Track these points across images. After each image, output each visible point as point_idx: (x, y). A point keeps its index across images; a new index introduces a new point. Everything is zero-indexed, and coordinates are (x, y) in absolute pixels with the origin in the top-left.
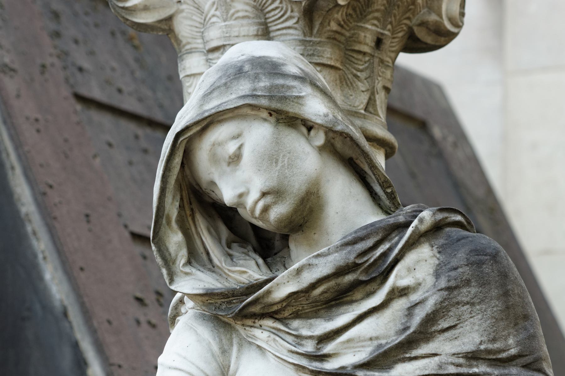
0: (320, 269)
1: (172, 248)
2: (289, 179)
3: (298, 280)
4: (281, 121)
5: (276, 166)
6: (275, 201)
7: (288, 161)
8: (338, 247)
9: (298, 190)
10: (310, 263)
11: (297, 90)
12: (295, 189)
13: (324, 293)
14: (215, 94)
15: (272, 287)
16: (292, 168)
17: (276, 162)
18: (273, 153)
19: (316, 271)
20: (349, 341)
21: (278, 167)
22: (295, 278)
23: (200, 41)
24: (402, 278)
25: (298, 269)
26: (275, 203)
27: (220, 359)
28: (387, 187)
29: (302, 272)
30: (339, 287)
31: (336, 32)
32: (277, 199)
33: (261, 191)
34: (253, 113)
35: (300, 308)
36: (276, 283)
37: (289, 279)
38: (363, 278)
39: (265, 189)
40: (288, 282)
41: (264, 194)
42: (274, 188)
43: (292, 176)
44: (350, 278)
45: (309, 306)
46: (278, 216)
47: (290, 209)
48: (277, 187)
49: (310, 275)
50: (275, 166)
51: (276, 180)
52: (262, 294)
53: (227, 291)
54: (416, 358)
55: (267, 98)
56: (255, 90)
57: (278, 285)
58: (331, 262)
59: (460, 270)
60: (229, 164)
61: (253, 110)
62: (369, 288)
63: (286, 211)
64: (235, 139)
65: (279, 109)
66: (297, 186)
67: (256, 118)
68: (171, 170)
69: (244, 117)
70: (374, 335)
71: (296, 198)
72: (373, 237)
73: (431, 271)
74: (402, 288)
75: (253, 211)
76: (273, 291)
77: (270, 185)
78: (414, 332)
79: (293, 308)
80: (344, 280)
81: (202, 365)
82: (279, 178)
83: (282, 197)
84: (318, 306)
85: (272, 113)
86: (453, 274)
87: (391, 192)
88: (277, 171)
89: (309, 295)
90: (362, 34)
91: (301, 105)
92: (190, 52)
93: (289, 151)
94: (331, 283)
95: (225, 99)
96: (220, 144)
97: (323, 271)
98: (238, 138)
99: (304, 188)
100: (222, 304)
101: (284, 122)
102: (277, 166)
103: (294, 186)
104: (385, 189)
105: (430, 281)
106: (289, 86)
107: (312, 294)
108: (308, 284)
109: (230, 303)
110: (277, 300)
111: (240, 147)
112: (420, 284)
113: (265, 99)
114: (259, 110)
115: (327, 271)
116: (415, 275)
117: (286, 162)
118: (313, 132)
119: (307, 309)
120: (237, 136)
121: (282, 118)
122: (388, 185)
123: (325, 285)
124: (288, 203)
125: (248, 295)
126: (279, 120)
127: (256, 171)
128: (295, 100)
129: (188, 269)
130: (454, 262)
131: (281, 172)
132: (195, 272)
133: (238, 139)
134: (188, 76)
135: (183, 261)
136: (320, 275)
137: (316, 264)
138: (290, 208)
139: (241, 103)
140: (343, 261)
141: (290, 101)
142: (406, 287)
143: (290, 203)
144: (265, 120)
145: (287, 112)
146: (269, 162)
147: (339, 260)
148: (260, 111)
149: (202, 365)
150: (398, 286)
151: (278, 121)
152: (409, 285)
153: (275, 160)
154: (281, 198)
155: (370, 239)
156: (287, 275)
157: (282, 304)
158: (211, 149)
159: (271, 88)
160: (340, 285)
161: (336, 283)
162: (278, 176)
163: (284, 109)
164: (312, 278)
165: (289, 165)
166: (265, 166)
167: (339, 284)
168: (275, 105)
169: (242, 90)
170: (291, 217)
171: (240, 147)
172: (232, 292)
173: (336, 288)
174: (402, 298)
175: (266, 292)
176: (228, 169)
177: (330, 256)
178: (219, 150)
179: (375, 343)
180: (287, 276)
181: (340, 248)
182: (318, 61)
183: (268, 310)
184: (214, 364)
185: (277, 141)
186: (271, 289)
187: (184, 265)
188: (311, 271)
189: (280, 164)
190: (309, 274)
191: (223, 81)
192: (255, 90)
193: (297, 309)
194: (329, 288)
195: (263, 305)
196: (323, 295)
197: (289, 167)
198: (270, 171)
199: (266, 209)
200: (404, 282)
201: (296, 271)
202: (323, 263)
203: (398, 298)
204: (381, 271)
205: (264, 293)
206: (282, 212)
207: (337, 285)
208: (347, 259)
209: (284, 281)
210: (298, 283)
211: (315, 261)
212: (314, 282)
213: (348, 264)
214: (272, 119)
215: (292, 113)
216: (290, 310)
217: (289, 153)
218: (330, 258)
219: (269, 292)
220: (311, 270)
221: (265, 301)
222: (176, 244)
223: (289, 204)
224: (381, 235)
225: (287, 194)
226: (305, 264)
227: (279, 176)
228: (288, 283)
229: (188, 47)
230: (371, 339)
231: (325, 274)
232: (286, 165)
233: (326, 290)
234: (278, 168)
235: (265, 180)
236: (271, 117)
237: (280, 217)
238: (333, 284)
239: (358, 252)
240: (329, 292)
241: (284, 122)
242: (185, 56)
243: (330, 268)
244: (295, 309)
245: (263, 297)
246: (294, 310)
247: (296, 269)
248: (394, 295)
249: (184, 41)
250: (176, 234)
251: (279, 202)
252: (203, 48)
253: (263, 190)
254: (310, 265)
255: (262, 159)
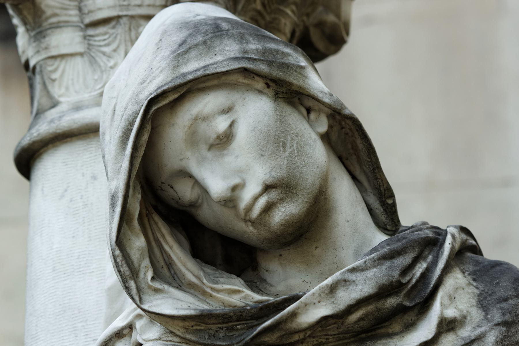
0: (360, 287)
1: (135, 255)
2: (301, 170)
3: (333, 300)
4: (280, 96)
5: (284, 152)
6: (283, 198)
7: (297, 147)
8: (375, 261)
9: (312, 185)
10: (346, 279)
11: (293, 59)
12: (308, 183)
13: (361, 319)
14: (193, 54)
15: (298, 308)
16: (302, 156)
17: (284, 147)
18: (278, 133)
19: (354, 290)
21: (286, 153)
22: (328, 297)
23: (75, 12)
25: (331, 286)
26: (282, 200)
28: (388, 196)
29: (337, 290)
30: (380, 313)
31: (259, 13)
32: (285, 195)
33: (264, 183)
34: (246, 81)
35: (324, 341)
36: (304, 302)
37: (320, 298)
38: (407, 303)
39: (269, 182)
40: (319, 302)
41: (267, 188)
42: (283, 180)
43: (304, 166)
44: (393, 302)
45: (335, 338)
46: (287, 218)
47: (303, 209)
48: (287, 179)
49: (347, 294)
50: (283, 151)
51: (284, 169)
52: (285, 317)
53: (233, 312)
55: (265, 63)
57: (306, 306)
58: (371, 279)
59: (510, 302)
60: (211, 147)
62: (408, 317)
63: (299, 212)
64: (224, 113)
65: (282, 78)
67: (249, 88)
68: (138, 148)
69: (233, 86)
71: (309, 196)
72: (410, 251)
73: (473, 302)
74: (449, 319)
75: (250, 208)
76: (299, 313)
77: (277, 175)
79: (314, 340)
80: (385, 304)
82: (288, 167)
83: (293, 193)
84: (345, 338)
85: (271, 84)
86: (504, 305)
87: (392, 203)
88: (285, 159)
89: (343, 321)
90: (283, 21)
91: (304, 77)
92: (57, 26)
93: (296, 135)
94: (371, 307)
95: (208, 61)
96: (205, 119)
97: (364, 290)
98: (228, 112)
99: (317, 183)
100: (218, 330)
101: (284, 98)
102: (285, 152)
103: (307, 179)
104: (386, 199)
105: (476, 314)
106: (284, 53)
107: (347, 321)
108: (346, 305)
109: (231, 329)
110: (304, 326)
112: (465, 317)
113: (264, 64)
114: (254, 79)
115: (369, 291)
116: (457, 306)
117: (295, 148)
119: (331, 342)
120: (228, 110)
121: (282, 92)
122: (390, 194)
123: (363, 309)
124: (300, 201)
125: (268, 316)
126: (278, 93)
127: (258, 157)
128: (298, 70)
129: (157, 285)
130: (501, 293)
131: (290, 159)
132: (168, 289)
133: (228, 114)
134: (54, 57)
135: (150, 274)
136: (360, 295)
137: (353, 280)
138: (304, 208)
139: (236, 65)
140: (385, 278)
141: (292, 70)
142: (453, 319)
143: (303, 201)
144: (261, 92)
145: (291, 84)
146: (275, 145)
147: (381, 277)
148: (254, 80)
150: (446, 317)
152: (455, 317)
153: (282, 143)
154: (291, 194)
155: (407, 254)
156: (319, 292)
157: (306, 333)
158: (192, 125)
159: (265, 52)
160: (381, 310)
161: (377, 308)
162: (287, 164)
163: (287, 80)
164: (350, 298)
165: (298, 152)
166: (270, 150)
167: (380, 309)
168: (276, 73)
169: (230, 51)
170: (303, 219)
171: (232, 125)
172: (240, 314)
173: (376, 314)
174: (450, 333)
175: (290, 314)
176: (209, 155)
177: (368, 272)
178: (203, 127)
180: (319, 294)
181: (377, 262)
183: (286, 340)
185: (281, 120)
186: (297, 311)
188: (347, 289)
189: (288, 150)
190: (346, 293)
191: (200, 38)
192: (246, 52)
193: (320, 341)
194: (368, 314)
195: (284, 333)
196: (359, 323)
197: (299, 154)
198: (277, 157)
199: (269, 208)
200: (451, 313)
201: (329, 289)
202: (362, 280)
203: (446, 333)
204: (424, 296)
205: (288, 315)
206: (293, 212)
207: (377, 311)
208: (390, 276)
209: (315, 301)
210: (332, 305)
211: (352, 277)
212: (353, 303)
213: (392, 282)
214: (270, 92)
215: (296, 85)
216: (309, 343)
217: (297, 136)
218: (370, 273)
219: (294, 315)
220: (347, 287)
221: (287, 327)
222: (139, 250)
223: (302, 203)
224: (417, 250)
225: (300, 189)
226: (340, 279)
227: (288, 165)
228: (319, 303)
229: (54, 20)
231: (366, 294)
232: (296, 151)
233: (364, 316)
234: (287, 154)
235: (271, 169)
236: (268, 90)
237: (290, 218)
238: (373, 308)
239: (400, 268)
240: (366, 319)
241: (284, 98)
242: (49, 31)
243: (372, 287)
244: (317, 341)
245: (285, 321)
246: (315, 343)
247: (330, 286)
248: (442, 328)
249: (49, 12)
250: (138, 236)
251: (288, 199)
252: (78, 22)
253: (267, 182)
254: (345, 281)
255: (267, 141)
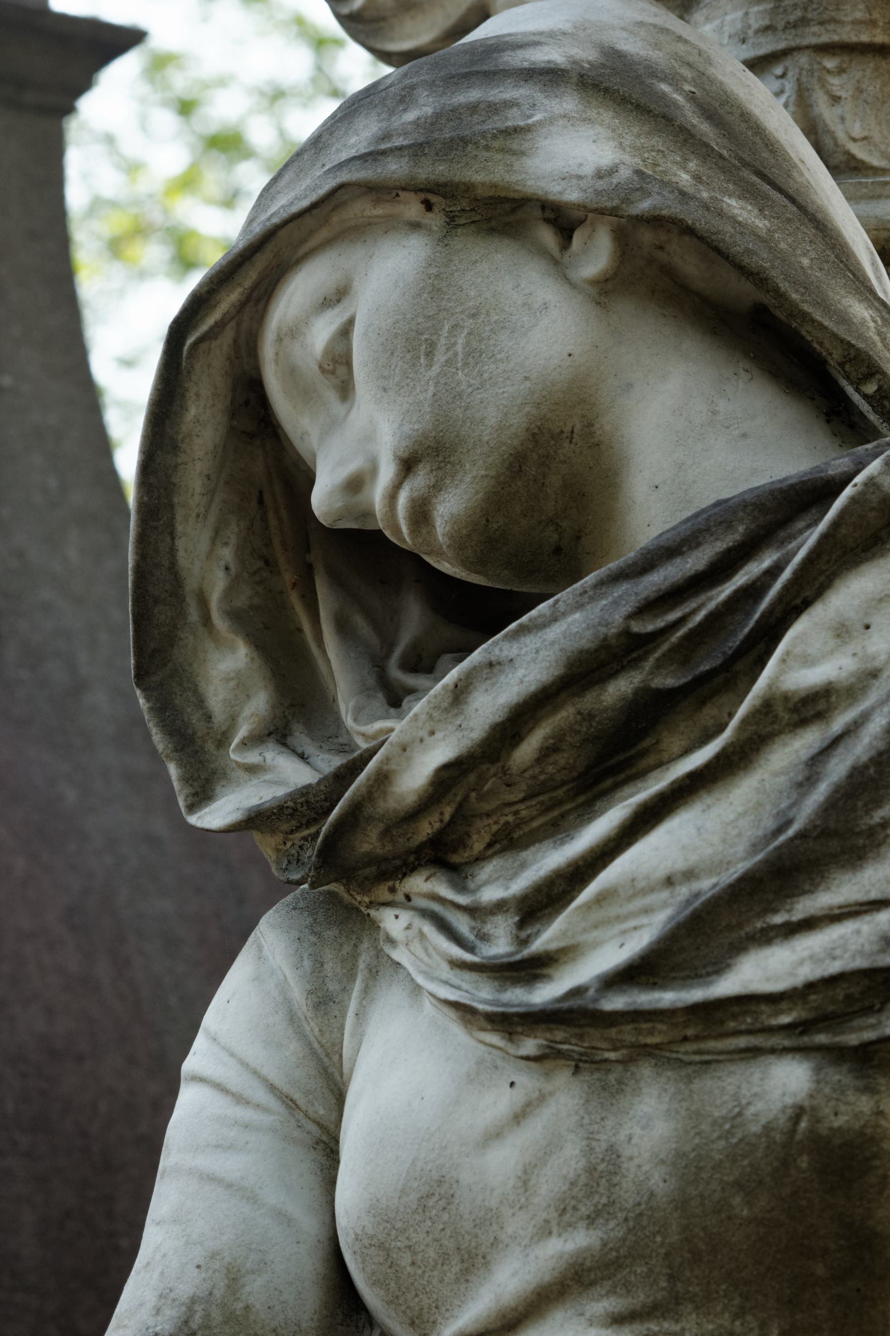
0: (520, 673)
1: (215, 695)
2: (468, 400)
3: (458, 722)
4: (462, 221)
5: (430, 366)
6: (437, 481)
7: (468, 343)
8: (586, 592)
9: (497, 430)
10: (493, 659)
11: (519, 113)
12: (486, 429)
13: (546, 753)
15: (387, 760)
16: (477, 363)
17: (429, 354)
18: (418, 324)
19: (507, 683)
20: (601, 899)
21: (433, 369)
22: (450, 715)
24: (808, 661)
25: (456, 686)
26: (437, 487)
27: (312, 1028)
28: (860, 376)
29: (470, 693)
30: (594, 724)
32: (440, 473)
33: (396, 456)
34: (379, 211)
35: (510, 818)
36: (396, 743)
37: (432, 723)
38: (668, 681)
40: (432, 733)
42: (426, 438)
43: (478, 389)
44: (623, 689)
45: (532, 806)
46: (447, 529)
47: (474, 499)
48: (433, 434)
49: (490, 698)
50: (427, 366)
51: (428, 410)
52: (364, 789)
53: (290, 799)
54: (809, 924)
55: (406, 152)
56: (386, 136)
57: (404, 750)
58: (553, 643)
61: (377, 202)
63: (466, 507)
64: (330, 306)
65: (442, 180)
66: (492, 416)
68: (180, 445)
70: (680, 865)
71: (490, 460)
72: (712, 539)
74: (803, 694)
76: (393, 771)
77: (414, 430)
78: (802, 835)
79: (491, 821)
80: (603, 698)
81: (256, 1055)
82: (436, 401)
83: (453, 465)
84: (560, 803)
85: (433, 199)
87: (877, 391)
88: (431, 382)
89: (503, 767)
91: (515, 154)
93: (474, 311)
97: (527, 679)
98: (339, 301)
99: (518, 421)
100: (303, 844)
101: (474, 222)
102: (431, 366)
103: (483, 419)
104: (858, 384)
106: (495, 104)
107: (511, 762)
108: (487, 727)
110: (411, 800)
111: (346, 331)
113: (402, 156)
114: (398, 198)
115: (539, 676)
116: (863, 647)
117: (459, 348)
118: (578, 239)
119: (533, 819)
121: (463, 210)
122: (864, 370)
123: (544, 725)
124: (468, 479)
126: (453, 217)
127: (379, 396)
128: (496, 144)
131: (442, 381)
132: (273, 760)
133: (340, 304)
136: (518, 694)
137: (510, 658)
138: (477, 492)
140: (589, 634)
141: (477, 147)
142: (818, 689)
143: (475, 478)
145: (469, 187)
146: (408, 356)
147: (578, 632)
148: (398, 201)
149: (256, 1055)
150: (787, 692)
151: (452, 223)
152: (830, 683)
153: (424, 347)
154: (449, 466)
155: (701, 549)
156: (427, 710)
157: (442, 814)
158: (277, 354)
160: (595, 716)
161: (579, 713)
162: (433, 396)
163: (457, 179)
164: (496, 707)
165: (468, 355)
166: (397, 372)
167: (589, 714)
169: (354, 145)
170: (485, 522)
171: (346, 331)
172: (303, 799)
173: (585, 729)
174: (808, 729)
175: (373, 778)
177: (558, 624)
179: (683, 891)
180: (428, 713)
181: (591, 593)
182: (825, 39)
183: (408, 840)
184: (294, 1048)
186: (385, 767)
187: (255, 740)
188: (493, 685)
189: (440, 357)
190: (490, 695)
193: (502, 822)
194: (562, 732)
195: (382, 826)
196: (551, 760)
197: (470, 360)
198: (412, 384)
201: (450, 694)
202: (531, 653)
203: (790, 731)
204: (730, 648)
205: (370, 783)
206: (454, 511)
207: (584, 719)
208: (602, 626)
209: (423, 733)
210: (457, 733)
212: (501, 719)
213: (605, 639)
215: (483, 184)
216: (483, 831)
217: (474, 316)
220: (494, 680)
221: (380, 811)
222: (227, 680)
223: (472, 483)
224: (741, 529)
225: (465, 450)
226: (477, 664)
227: (437, 397)
228: (432, 738)
230: (669, 881)
231: (533, 688)
232: (461, 356)
233: (552, 741)
234: (436, 369)
235: (402, 417)
236: (430, 215)
237: (452, 528)
238: (569, 716)
239: (643, 595)
240: (565, 747)
241: (474, 222)
243: (548, 665)
244: (496, 823)
245: (370, 798)
246: (495, 828)
247: (452, 687)
248: (773, 723)
250: (233, 649)
251: (446, 480)
253: (399, 454)
254: (491, 665)
255: (390, 352)
